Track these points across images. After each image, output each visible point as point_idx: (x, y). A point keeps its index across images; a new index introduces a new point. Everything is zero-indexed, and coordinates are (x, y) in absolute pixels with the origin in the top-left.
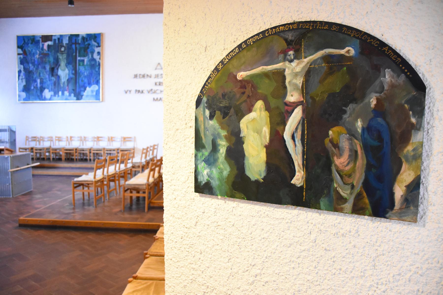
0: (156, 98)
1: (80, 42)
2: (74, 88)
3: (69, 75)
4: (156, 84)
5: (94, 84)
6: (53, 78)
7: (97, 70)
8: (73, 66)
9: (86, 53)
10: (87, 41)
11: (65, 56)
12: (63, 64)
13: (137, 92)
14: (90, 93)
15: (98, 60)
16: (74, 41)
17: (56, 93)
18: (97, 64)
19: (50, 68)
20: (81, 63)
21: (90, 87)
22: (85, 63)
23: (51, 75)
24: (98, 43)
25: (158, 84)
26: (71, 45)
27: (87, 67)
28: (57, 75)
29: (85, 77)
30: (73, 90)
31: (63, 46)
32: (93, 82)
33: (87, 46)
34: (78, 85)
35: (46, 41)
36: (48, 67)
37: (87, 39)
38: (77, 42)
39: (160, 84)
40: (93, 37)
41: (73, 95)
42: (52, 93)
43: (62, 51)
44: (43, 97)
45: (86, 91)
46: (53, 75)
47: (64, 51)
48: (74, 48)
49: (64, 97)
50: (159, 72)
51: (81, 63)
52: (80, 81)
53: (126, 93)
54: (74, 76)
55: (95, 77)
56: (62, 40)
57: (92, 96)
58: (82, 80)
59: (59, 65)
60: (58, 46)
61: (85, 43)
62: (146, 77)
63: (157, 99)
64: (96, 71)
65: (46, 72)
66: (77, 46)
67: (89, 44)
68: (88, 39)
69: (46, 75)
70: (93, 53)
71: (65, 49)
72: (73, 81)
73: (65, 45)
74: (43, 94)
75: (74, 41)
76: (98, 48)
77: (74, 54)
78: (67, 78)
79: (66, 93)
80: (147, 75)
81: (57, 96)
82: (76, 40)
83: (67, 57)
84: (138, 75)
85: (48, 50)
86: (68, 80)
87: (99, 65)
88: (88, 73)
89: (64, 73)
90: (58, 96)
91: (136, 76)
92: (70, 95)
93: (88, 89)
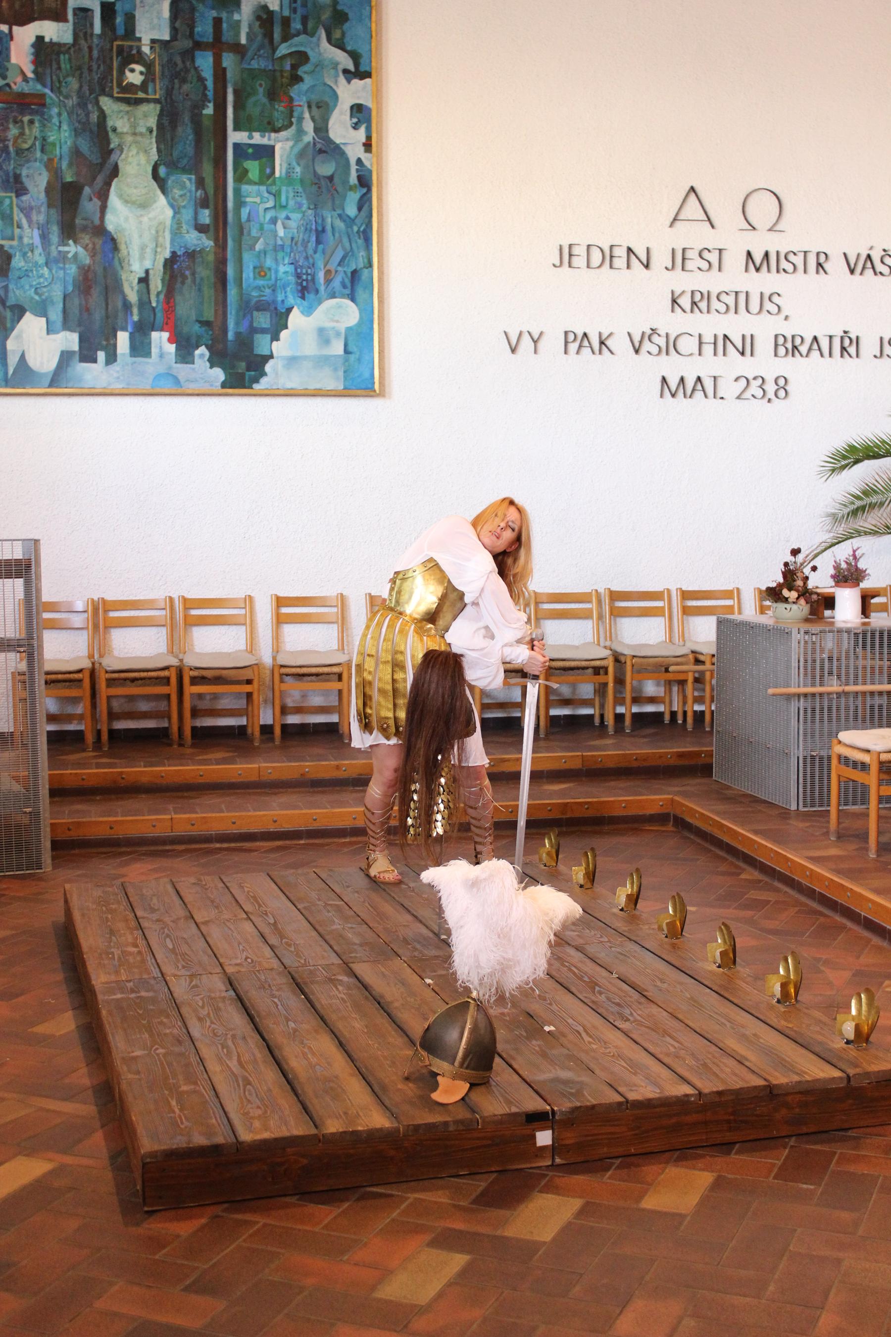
0: (673, 383)
1: (243, 41)
2: (209, 314)
3: (176, 232)
4: (674, 301)
5: (333, 296)
6: (72, 248)
7: (351, 210)
8: (200, 183)
9: (280, 107)
10: (286, 38)
11: (148, 116)
12: (136, 162)
13: (573, 347)
14: (310, 348)
15: (355, 152)
16: (204, 29)
17: (94, 343)
18: (353, 179)
19: (48, 190)
20: (253, 168)
21: (308, 311)
22: (279, 170)
23: (55, 229)
24: (355, 56)
25: (685, 301)
26: (189, 55)
27: (286, 194)
28: (100, 230)
29: (278, 249)
30: (207, 324)
31: (130, 57)
32: (328, 281)
33: (288, 67)
34: (232, 292)
35: (22, 23)
36: (37, 181)
37: (286, 22)
38: (227, 36)
39: (694, 303)
40: (326, 15)
41: (202, 351)
42: (71, 340)
43: (131, 87)
44: (13, 361)
45: (284, 334)
46: (69, 231)
47: (144, 87)
48: (208, 73)
49: (151, 366)
50: (694, 236)
51: (253, 168)
52: (248, 273)
53: (513, 351)
54: (207, 243)
55: (339, 254)
56: (130, 19)
57: (322, 361)
58: (260, 271)
59: (115, 172)
60: (105, 58)
61: (274, 50)
62: (621, 262)
63: (682, 379)
64: (349, 221)
65: (27, 211)
66: (228, 60)
67: (301, 58)
68: (297, 25)
69: (30, 237)
70: (323, 108)
71: (149, 75)
72: (205, 272)
73: (146, 50)
74: (11, 344)
75: (204, 29)
76: (355, 82)
77: (209, 110)
78: (167, 255)
79: (160, 339)
80: (630, 250)
81: (101, 355)
82: (217, 22)
83: (160, 126)
84: (580, 251)
85: (39, 77)
86: (170, 263)
87: (364, 182)
88: (293, 224)
89: (144, 221)
90: (112, 358)
91: (566, 256)
92: (185, 354)
93: (296, 318)
